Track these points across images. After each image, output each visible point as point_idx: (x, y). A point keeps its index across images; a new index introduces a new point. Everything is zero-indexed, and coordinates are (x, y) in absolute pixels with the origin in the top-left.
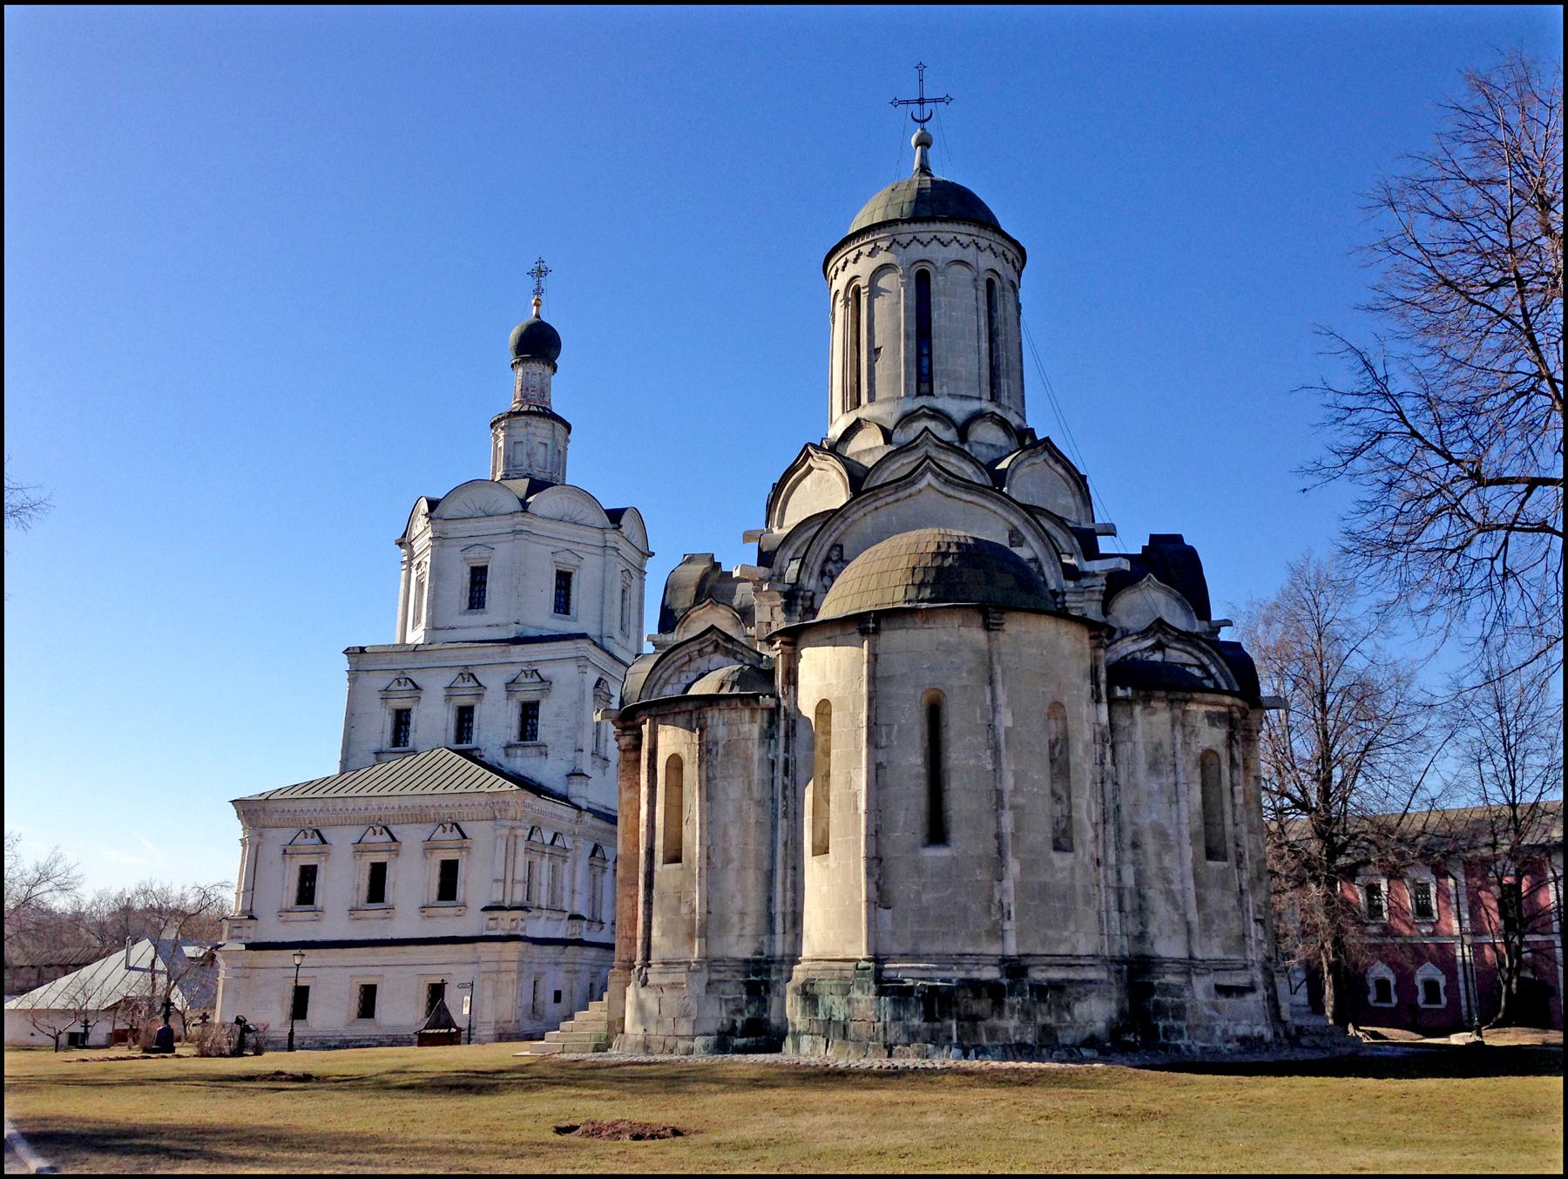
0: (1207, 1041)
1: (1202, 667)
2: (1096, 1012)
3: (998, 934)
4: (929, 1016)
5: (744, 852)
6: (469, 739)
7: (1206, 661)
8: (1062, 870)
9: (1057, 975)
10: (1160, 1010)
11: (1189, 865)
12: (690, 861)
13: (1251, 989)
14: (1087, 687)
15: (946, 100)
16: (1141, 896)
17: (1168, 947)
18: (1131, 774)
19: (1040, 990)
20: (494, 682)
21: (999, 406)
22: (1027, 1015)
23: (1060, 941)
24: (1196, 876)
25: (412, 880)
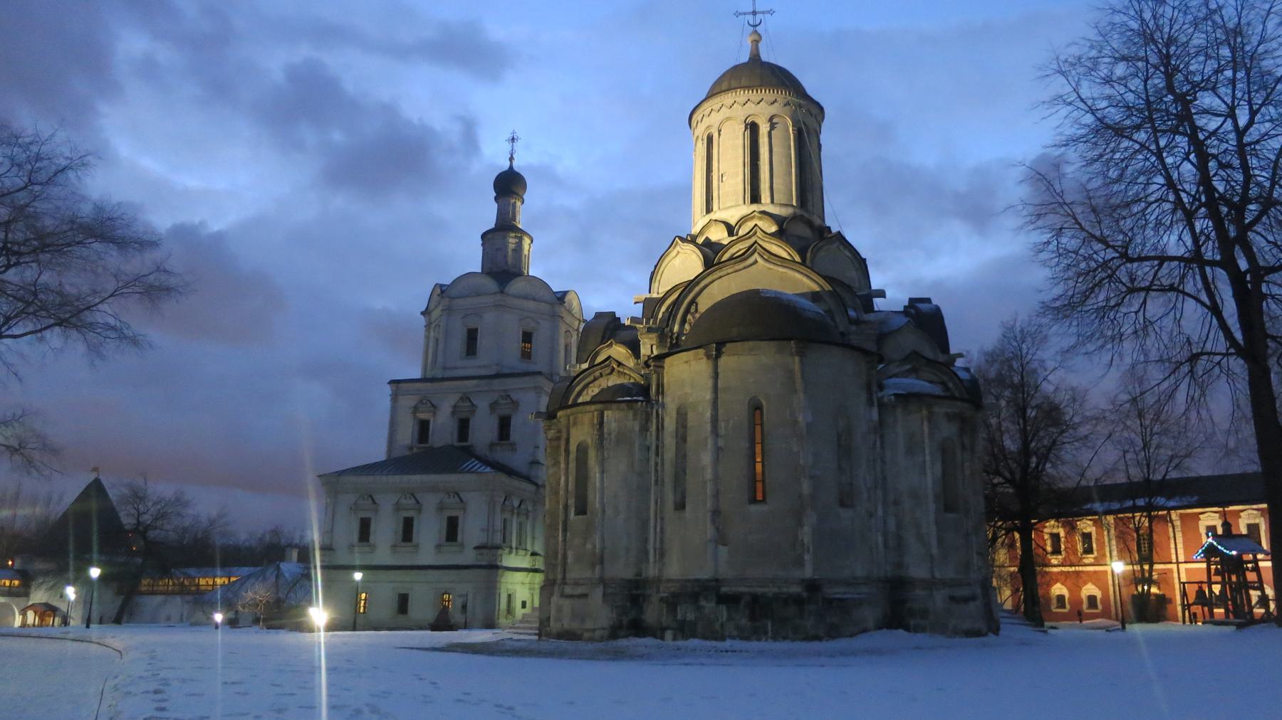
3: (800, 563)
4: (753, 617)
6: (466, 440)
7: (945, 378)
11: (932, 517)
13: (973, 598)
14: (863, 397)
15: (771, 12)
17: (918, 571)
19: (829, 602)
20: (482, 404)
21: (807, 211)
24: (937, 523)
25: (429, 530)
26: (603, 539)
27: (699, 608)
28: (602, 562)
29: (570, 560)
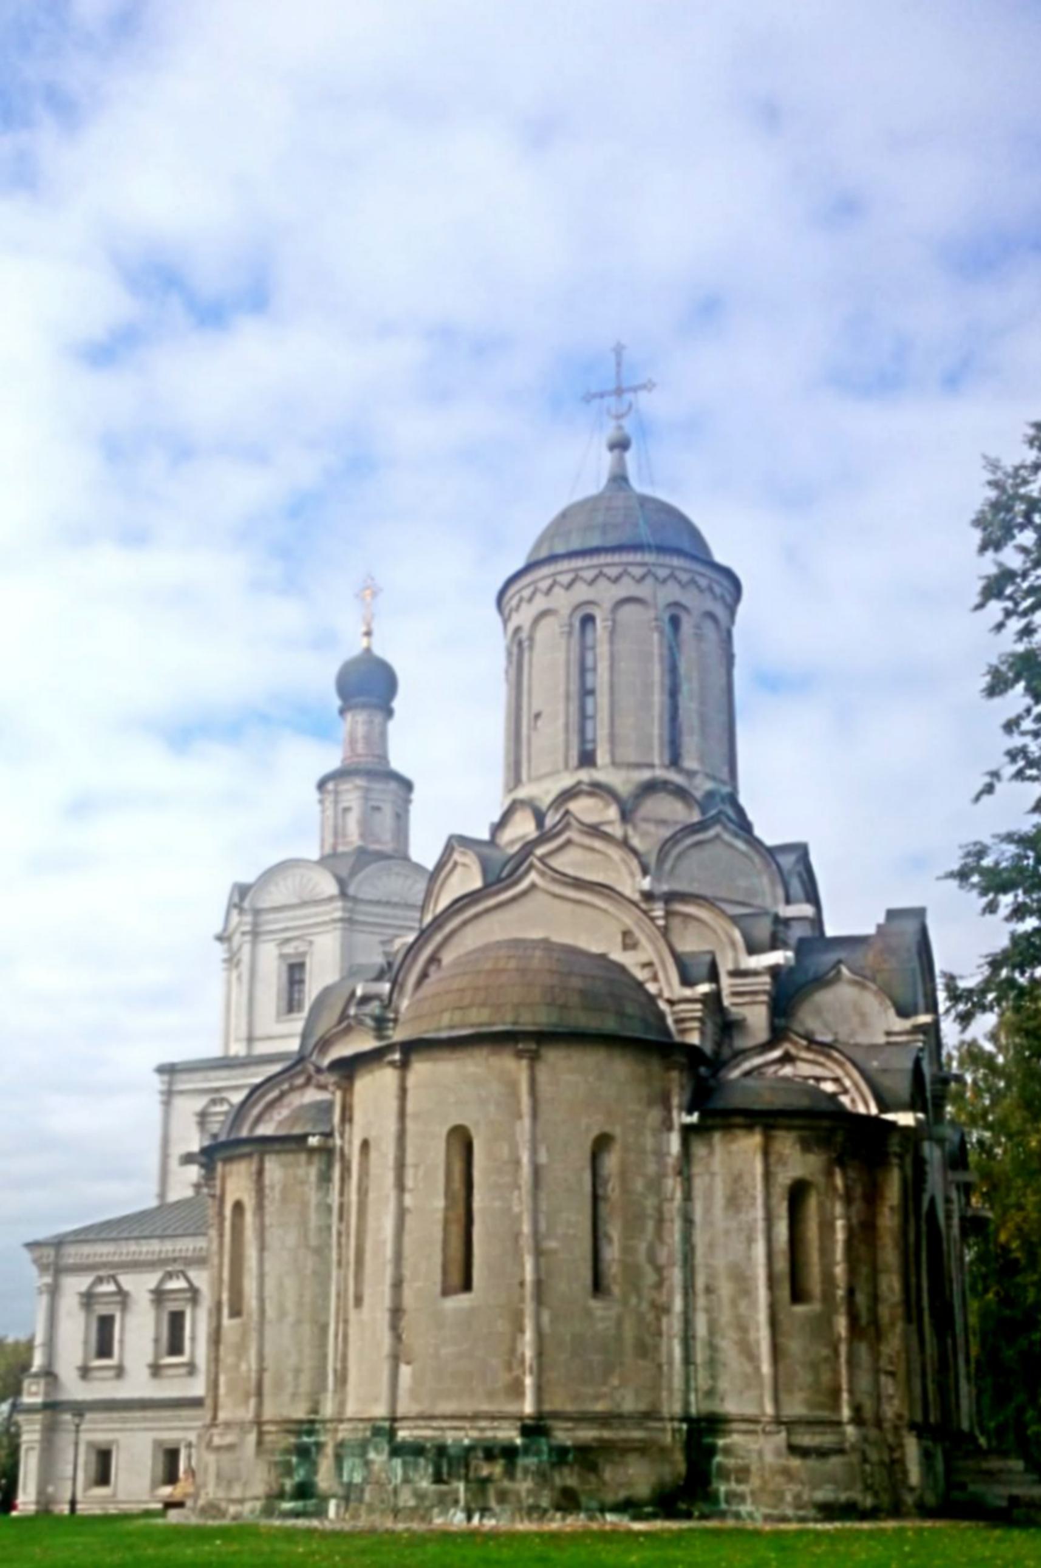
0: (775, 1507)
1: (836, 1080)
2: (639, 1477)
3: (516, 1390)
5: (300, 1304)
8: (603, 1319)
9: (587, 1434)
10: (724, 1474)
12: (250, 1315)
16: (712, 1347)
18: (708, 1210)
19: (561, 1454)
21: (680, 770)
22: (542, 1477)
23: (597, 1398)
24: (774, 1322)
26: (261, 1357)
27: (367, 1464)
28: (259, 1393)
29: (222, 1390)
